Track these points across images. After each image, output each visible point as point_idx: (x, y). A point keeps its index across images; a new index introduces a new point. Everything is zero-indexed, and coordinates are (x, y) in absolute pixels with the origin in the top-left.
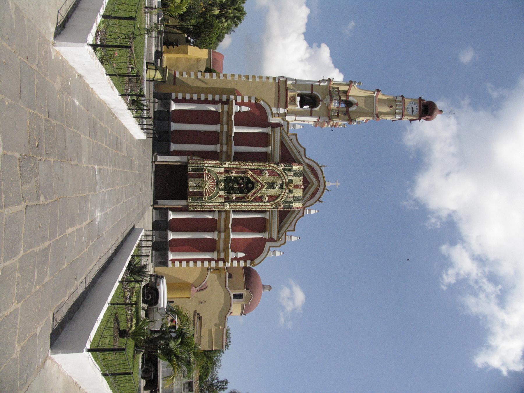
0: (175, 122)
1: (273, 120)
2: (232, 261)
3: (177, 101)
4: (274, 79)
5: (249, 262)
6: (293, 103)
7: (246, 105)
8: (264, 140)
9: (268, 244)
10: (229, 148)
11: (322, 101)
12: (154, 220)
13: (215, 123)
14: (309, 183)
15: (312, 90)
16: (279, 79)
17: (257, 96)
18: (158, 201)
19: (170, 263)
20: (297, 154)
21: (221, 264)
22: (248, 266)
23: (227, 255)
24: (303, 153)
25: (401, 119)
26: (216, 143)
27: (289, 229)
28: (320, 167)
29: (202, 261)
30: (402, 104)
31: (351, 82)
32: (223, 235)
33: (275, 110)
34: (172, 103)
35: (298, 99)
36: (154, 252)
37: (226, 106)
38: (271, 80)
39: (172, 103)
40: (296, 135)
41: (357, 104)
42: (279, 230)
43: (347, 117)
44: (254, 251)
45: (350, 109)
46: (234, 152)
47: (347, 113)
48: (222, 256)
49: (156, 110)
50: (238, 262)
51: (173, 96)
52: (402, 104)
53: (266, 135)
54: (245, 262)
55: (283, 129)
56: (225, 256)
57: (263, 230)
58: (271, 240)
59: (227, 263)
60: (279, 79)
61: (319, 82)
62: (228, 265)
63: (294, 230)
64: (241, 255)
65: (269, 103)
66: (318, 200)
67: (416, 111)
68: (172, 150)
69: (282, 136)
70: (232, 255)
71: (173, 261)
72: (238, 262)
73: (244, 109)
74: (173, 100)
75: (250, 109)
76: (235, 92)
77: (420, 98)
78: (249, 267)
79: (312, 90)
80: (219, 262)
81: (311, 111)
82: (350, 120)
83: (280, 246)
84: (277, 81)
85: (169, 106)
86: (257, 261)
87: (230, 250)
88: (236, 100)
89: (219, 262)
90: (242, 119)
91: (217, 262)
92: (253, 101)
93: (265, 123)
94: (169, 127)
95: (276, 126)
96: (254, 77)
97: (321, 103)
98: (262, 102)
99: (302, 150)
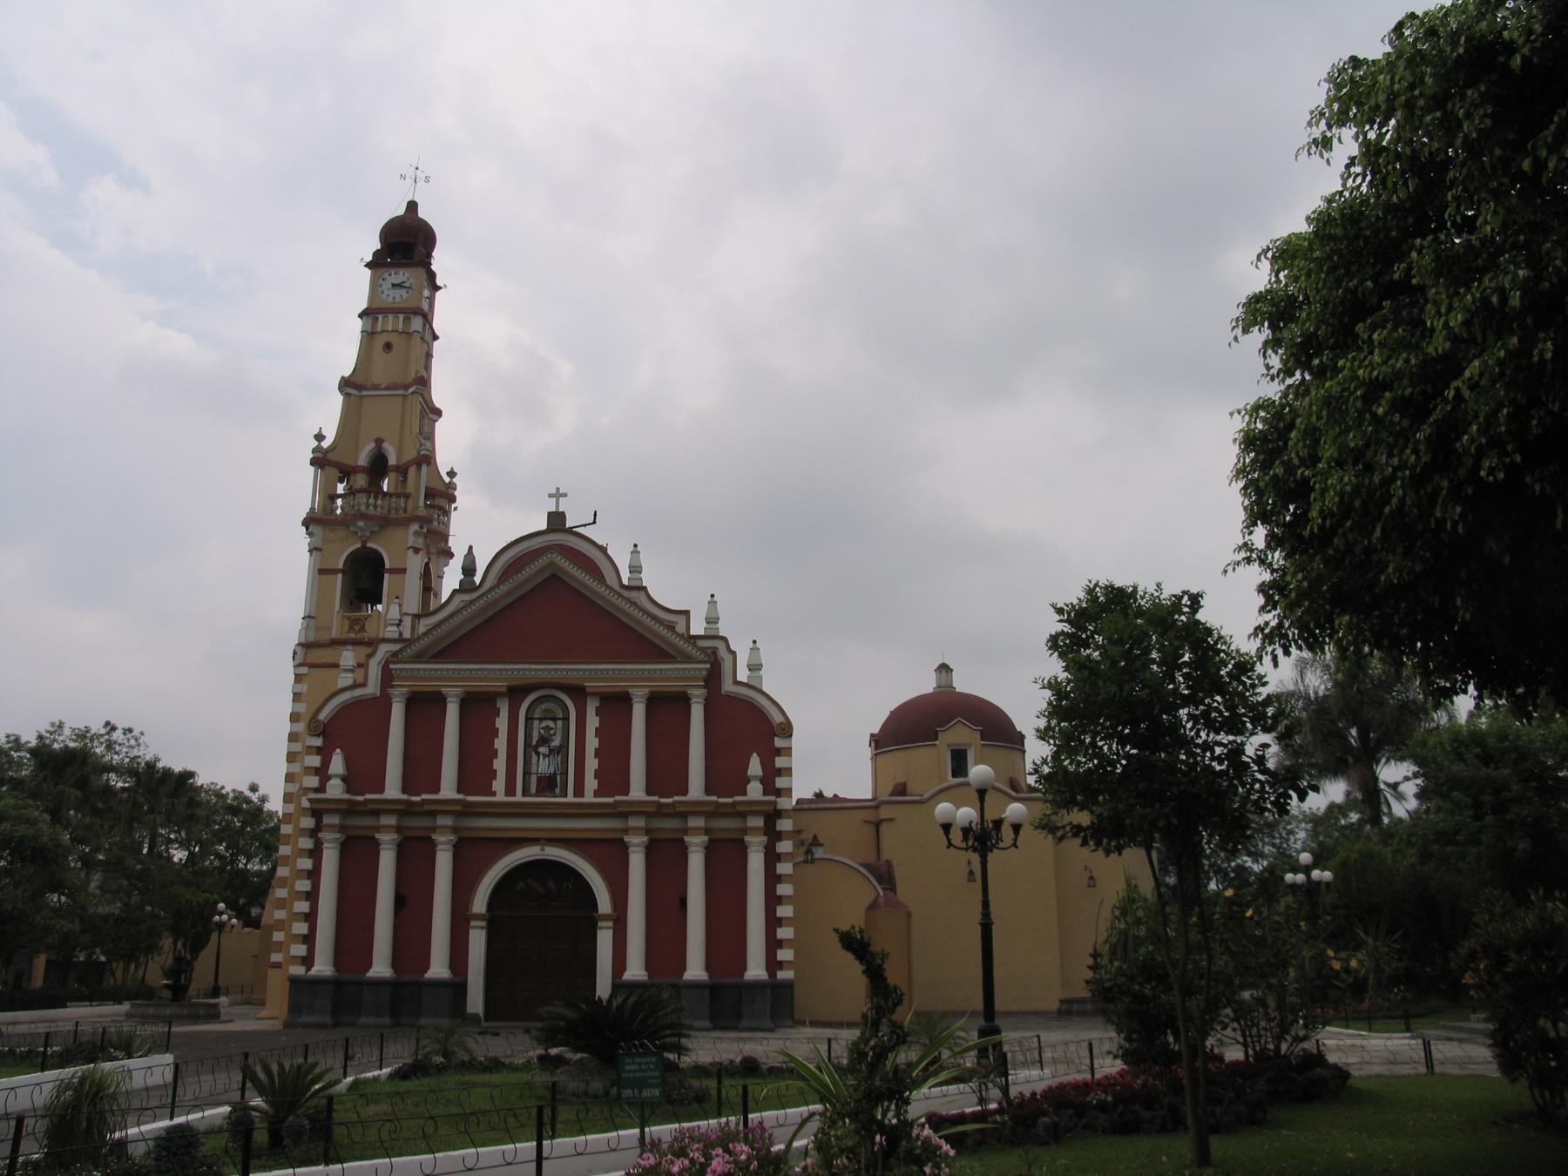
0: (427, 967)
3: (308, 961)
4: (298, 678)
7: (326, 763)
8: (424, 706)
9: (728, 687)
10: (331, 806)
11: (364, 543)
12: (707, 1024)
13: (374, 848)
14: (554, 576)
15: (334, 571)
16: (300, 665)
19: (784, 975)
23: (752, 809)
24: (467, 597)
26: (432, 846)
29: (772, 879)
32: (696, 822)
33: (345, 680)
34: (314, 971)
36: (744, 1023)
37: (327, 820)
38: (303, 688)
39: (314, 971)
41: (379, 442)
42: (688, 659)
43: (412, 470)
45: (392, 461)
46: (459, 791)
48: (758, 822)
49: (328, 1019)
51: (298, 970)
55: (395, 654)
56: (755, 813)
57: (683, 700)
58: (714, 677)
60: (300, 665)
63: (686, 613)
64: (755, 767)
65: (329, 693)
67: (402, 275)
69: (417, 658)
70: (755, 791)
71: (773, 965)
73: (337, 764)
74: (309, 969)
77: (368, 265)
79: (334, 571)
81: (392, 571)
83: (734, 653)
84: (304, 670)
85: (318, 982)
86: (777, 718)
90: (364, 774)
92: (318, 742)
93: (381, 705)
94: (379, 983)
95: (387, 678)
97: (370, 545)
98: (323, 716)
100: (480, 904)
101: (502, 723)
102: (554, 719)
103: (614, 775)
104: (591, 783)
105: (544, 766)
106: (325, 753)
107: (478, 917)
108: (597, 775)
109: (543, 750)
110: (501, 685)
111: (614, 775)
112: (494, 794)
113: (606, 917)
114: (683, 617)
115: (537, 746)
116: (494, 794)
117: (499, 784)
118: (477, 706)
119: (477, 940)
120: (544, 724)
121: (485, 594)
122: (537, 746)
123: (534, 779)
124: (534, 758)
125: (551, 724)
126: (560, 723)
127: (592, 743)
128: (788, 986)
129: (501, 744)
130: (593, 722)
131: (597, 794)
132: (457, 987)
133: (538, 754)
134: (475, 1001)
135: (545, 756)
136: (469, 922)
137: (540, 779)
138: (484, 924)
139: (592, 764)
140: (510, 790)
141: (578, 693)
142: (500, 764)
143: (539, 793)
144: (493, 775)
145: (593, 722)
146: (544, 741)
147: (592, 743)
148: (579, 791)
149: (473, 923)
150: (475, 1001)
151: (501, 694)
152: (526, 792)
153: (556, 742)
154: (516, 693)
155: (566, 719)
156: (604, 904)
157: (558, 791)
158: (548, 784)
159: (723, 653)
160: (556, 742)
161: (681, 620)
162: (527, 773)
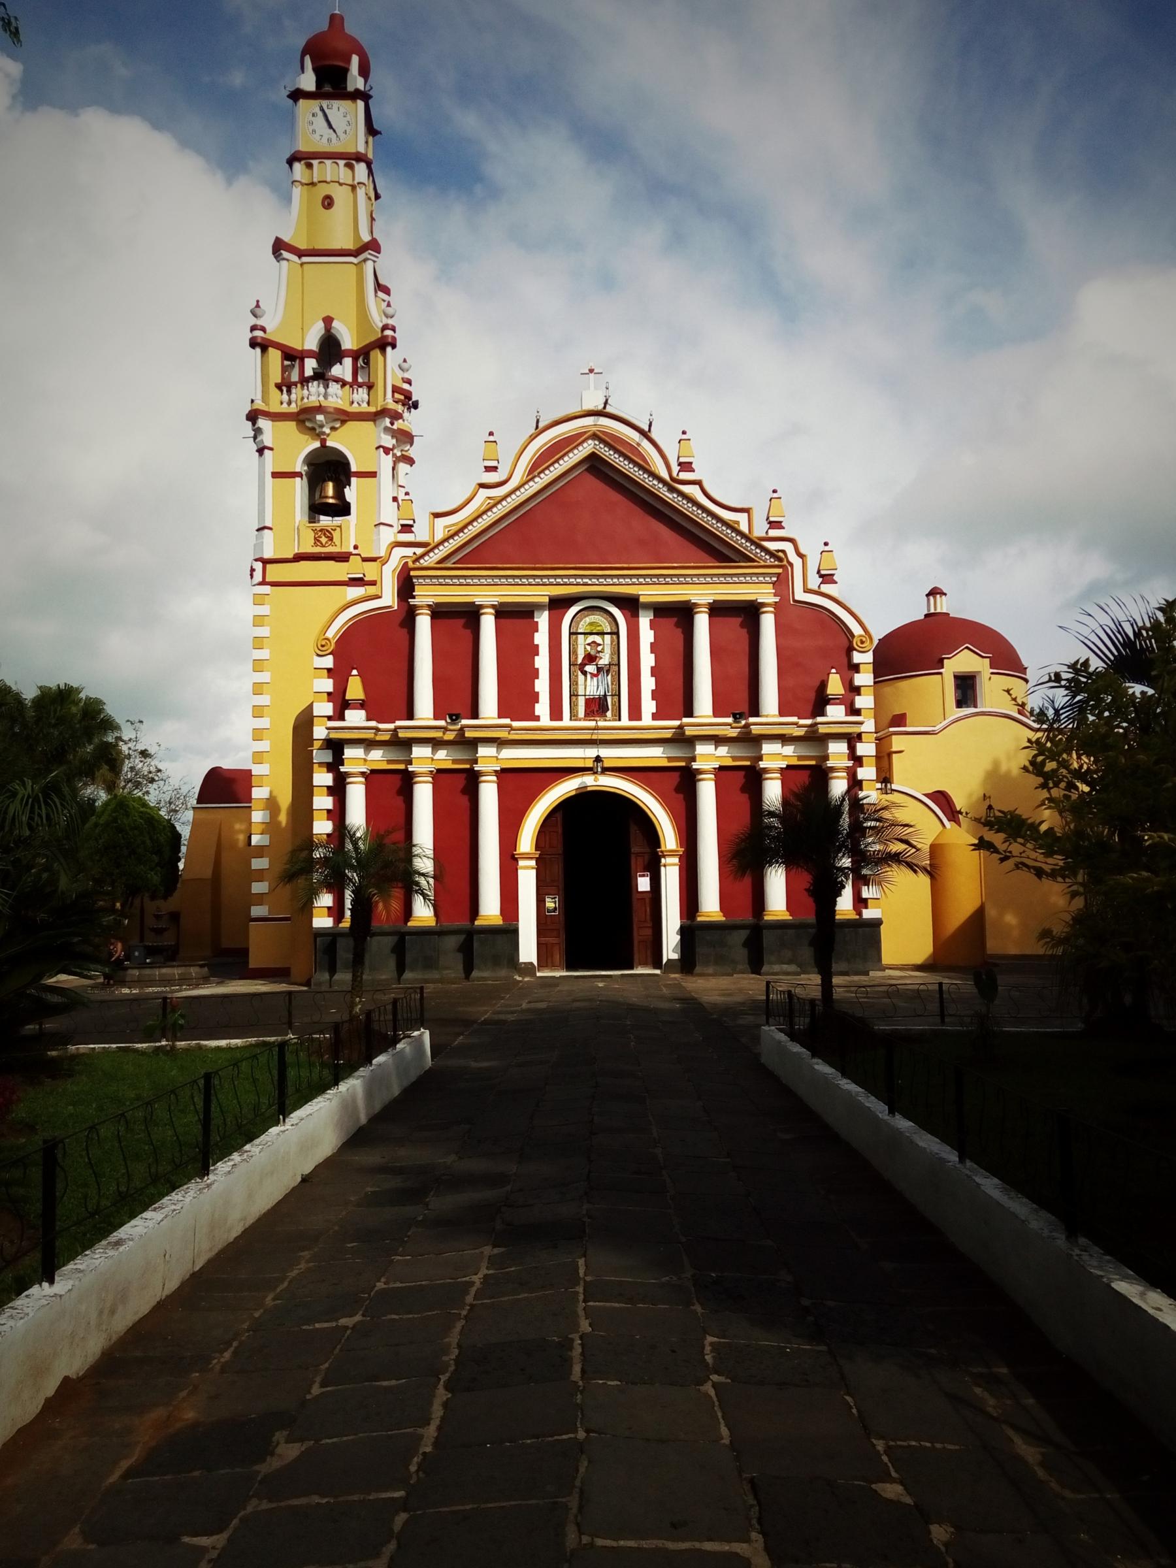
1: (389, 598)
2: (857, 712)
5: (857, 658)
6: (336, 535)
17: (311, 648)
18: (665, 960)
19: (867, 914)
20: (499, 511)
21: (866, 749)
22: (868, 657)
25: (369, 164)
27: (744, 528)
28: (539, 431)
30: (315, 162)
31: (253, 344)
35: (325, 521)
40: (437, 515)
44: (821, 640)
47: (362, 356)
50: (857, 690)
52: (315, 162)
53: (439, 613)
54: (856, 668)
57: (750, 612)
59: (863, 728)
61: (261, 451)
62: (869, 726)
64: (835, 686)
66: (645, 434)
68: (499, 921)
71: (860, 902)
72: (857, 690)
75: (355, 672)
76: (304, 723)
78: (876, 653)
80: (859, 753)
82: (384, 344)
86: (857, 630)
87: (819, 719)
88: (330, 718)
89: (859, 753)
91: (858, 761)
96: (258, 665)
99: (484, 493)
100: (526, 841)
101: (542, 638)
102: (602, 634)
103: (677, 696)
104: (648, 706)
105: (592, 687)
106: (338, 674)
107: (527, 857)
108: (655, 695)
109: (590, 668)
110: (539, 594)
111: (677, 696)
112: (537, 719)
113: (672, 853)
114: (746, 515)
115: (583, 665)
116: (537, 719)
117: (542, 708)
118: (515, 617)
119: (527, 879)
120: (591, 639)
121: (513, 492)
122: (583, 665)
123: (581, 702)
124: (581, 677)
125: (598, 639)
126: (608, 638)
127: (647, 660)
128: (876, 924)
129: (542, 662)
130: (647, 636)
131: (655, 717)
132: (509, 932)
133: (585, 673)
134: (528, 951)
135: (593, 675)
136: (516, 860)
137: (589, 702)
138: (533, 863)
139: (648, 683)
140: (556, 714)
141: (630, 605)
142: (542, 685)
143: (589, 714)
144: (535, 697)
145: (647, 636)
146: (590, 658)
147: (647, 660)
148: (635, 713)
149: (521, 863)
150: (528, 951)
151: (539, 607)
152: (574, 716)
153: (605, 660)
154: (558, 605)
155: (617, 634)
156: (669, 838)
157: (609, 714)
158: (597, 707)
159: (792, 557)
160: (605, 660)
161: (742, 518)
162: (573, 695)
